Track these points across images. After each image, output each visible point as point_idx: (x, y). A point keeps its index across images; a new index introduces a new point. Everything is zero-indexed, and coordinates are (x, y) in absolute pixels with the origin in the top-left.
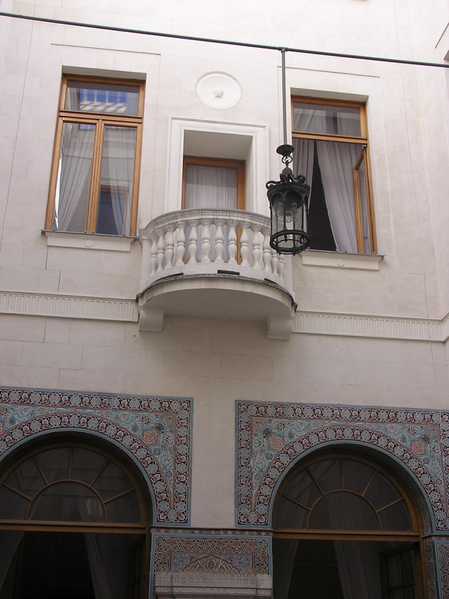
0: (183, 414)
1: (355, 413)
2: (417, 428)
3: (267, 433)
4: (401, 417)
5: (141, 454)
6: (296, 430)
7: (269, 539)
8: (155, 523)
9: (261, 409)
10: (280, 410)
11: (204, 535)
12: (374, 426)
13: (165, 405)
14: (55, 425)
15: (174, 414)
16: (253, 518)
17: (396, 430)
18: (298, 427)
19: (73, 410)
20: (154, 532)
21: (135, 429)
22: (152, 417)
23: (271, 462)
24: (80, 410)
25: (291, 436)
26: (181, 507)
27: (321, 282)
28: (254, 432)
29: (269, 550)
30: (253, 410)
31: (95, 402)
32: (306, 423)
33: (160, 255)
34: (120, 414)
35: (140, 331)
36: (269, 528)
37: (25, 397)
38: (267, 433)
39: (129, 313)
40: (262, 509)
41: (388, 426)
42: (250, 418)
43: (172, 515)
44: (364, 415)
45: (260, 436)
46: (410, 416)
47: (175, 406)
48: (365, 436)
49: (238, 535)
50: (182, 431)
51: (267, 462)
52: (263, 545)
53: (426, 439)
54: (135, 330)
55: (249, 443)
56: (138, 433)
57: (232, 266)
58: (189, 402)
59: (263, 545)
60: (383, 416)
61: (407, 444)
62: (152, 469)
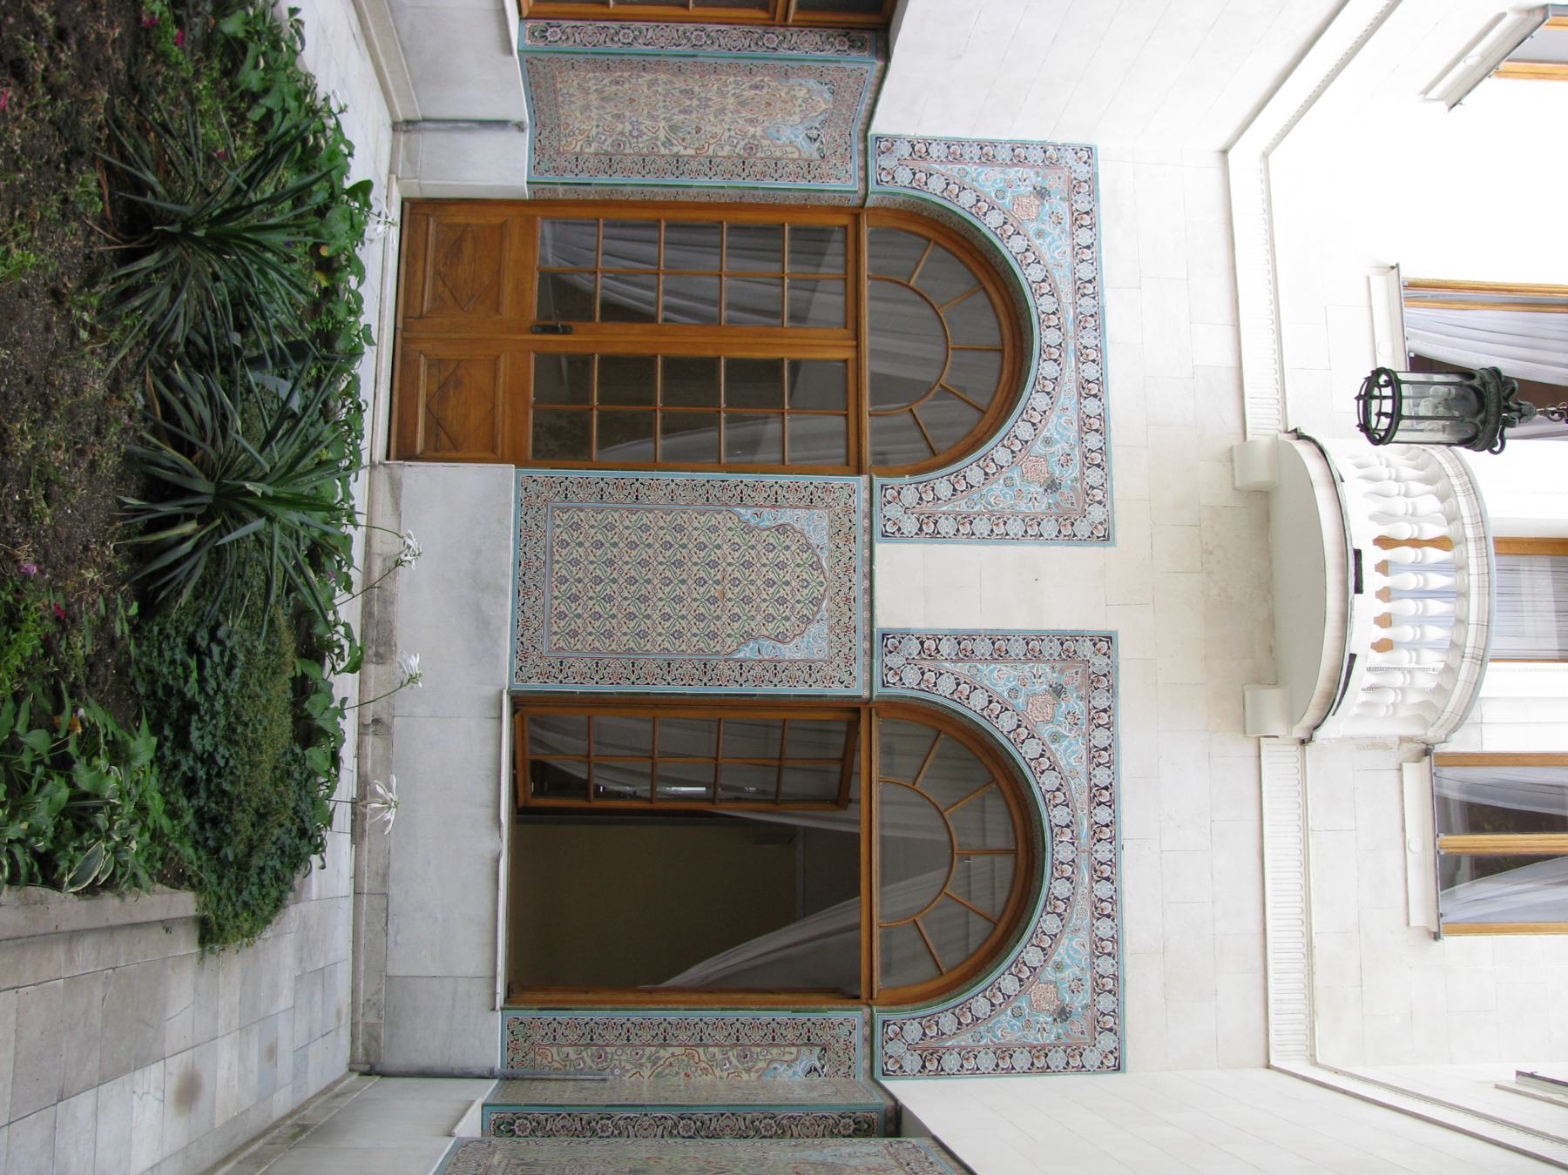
0: (1083, 529)
1: (1106, 872)
2: (1083, 998)
3: (1058, 691)
4: (1105, 965)
5: (1002, 456)
6: (1067, 748)
7: (859, 690)
8: (878, 481)
9: (1102, 681)
10: (1102, 717)
11: (862, 568)
12: (1082, 906)
13: (1095, 494)
14: (1040, 305)
15: (1078, 515)
16: (895, 661)
17: (1077, 952)
18: (1074, 752)
19: (1071, 333)
20: (864, 479)
21: (1048, 441)
22: (1073, 471)
23: (1000, 697)
24: (1071, 347)
25: (1056, 738)
26: (910, 525)
27: (1379, 834)
28: (1058, 666)
29: (837, 690)
30: (1100, 663)
31: (1090, 371)
32: (1082, 768)
33: (1385, 473)
34: (1072, 414)
35: (1231, 449)
36: (878, 690)
37: (1086, 252)
38: (1058, 691)
39: (1263, 424)
40: (911, 677)
41: (1084, 936)
42: (1085, 661)
43: (893, 511)
44: (1103, 889)
45: (1054, 677)
46: (1109, 985)
47: (1097, 513)
48: (1061, 889)
49: (863, 629)
50: (1050, 528)
51: (1002, 690)
52: (846, 677)
53: (1063, 1014)
54: (1231, 438)
55: (1037, 657)
56: (1038, 447)
57: (1372, 580)
58: (1106, 538)
59: (846, 677)
60: (1104, 928)
61: (1049, 973)
62: (975, 475)
